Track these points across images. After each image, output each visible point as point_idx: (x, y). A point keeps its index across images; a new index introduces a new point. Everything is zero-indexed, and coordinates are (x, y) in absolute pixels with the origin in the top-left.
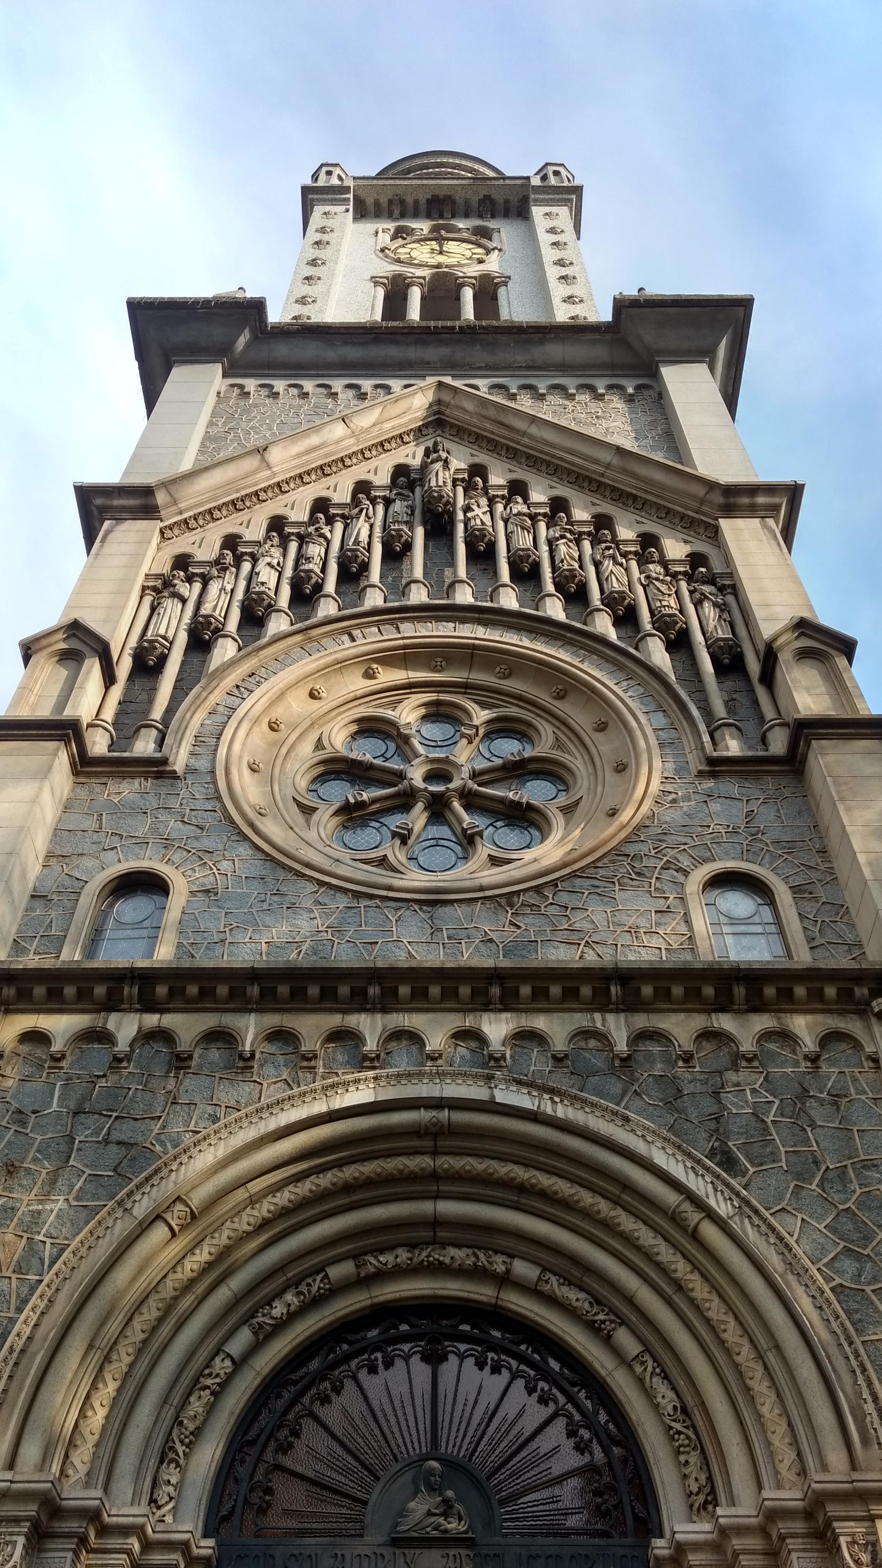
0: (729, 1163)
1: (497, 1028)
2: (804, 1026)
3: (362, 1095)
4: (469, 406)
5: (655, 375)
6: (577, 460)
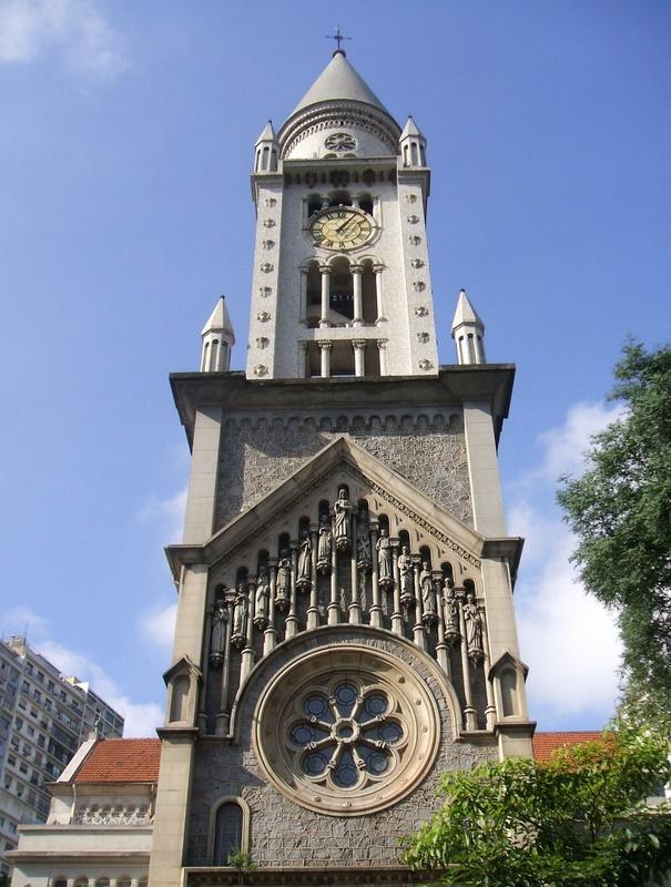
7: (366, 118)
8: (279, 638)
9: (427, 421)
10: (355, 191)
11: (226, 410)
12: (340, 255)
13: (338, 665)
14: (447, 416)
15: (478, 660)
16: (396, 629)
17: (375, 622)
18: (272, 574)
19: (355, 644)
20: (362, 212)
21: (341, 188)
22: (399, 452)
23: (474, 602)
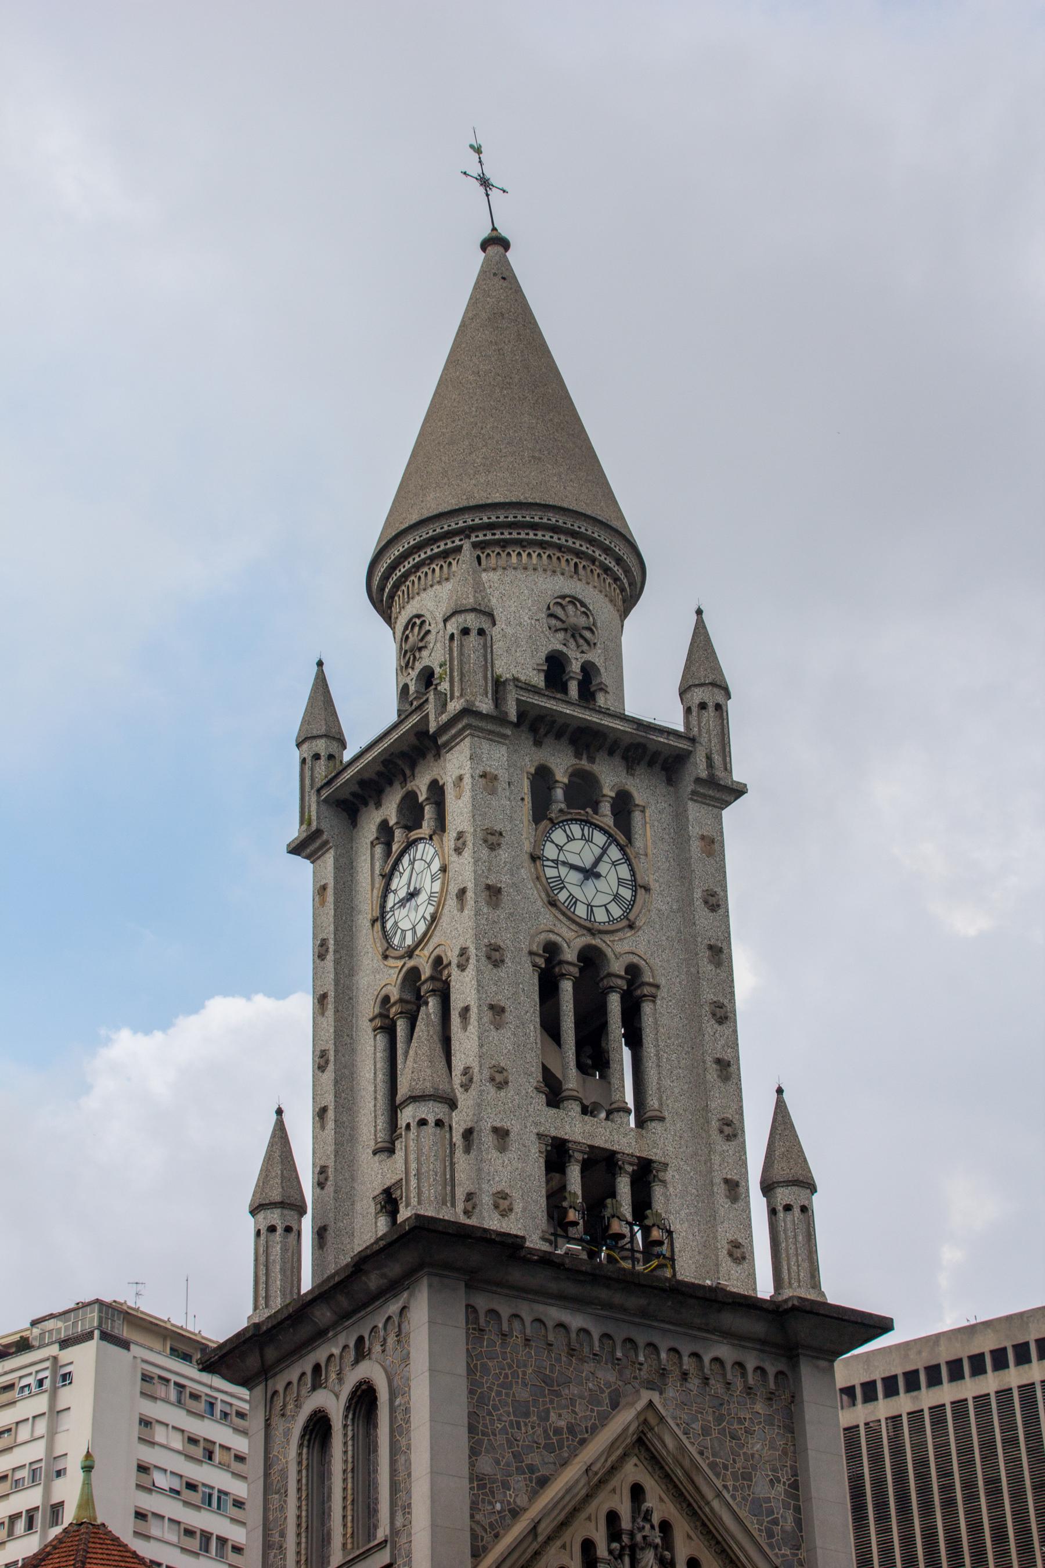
5: (795, 1366)
6: (743, 1558)
7: (612, 564)
9: (744, 1374)
10: (610, 778)
11: (469, 1286)
14: (771, 1370)
20: (622, 839)
21: (584, 763)
22: (706, 1431)
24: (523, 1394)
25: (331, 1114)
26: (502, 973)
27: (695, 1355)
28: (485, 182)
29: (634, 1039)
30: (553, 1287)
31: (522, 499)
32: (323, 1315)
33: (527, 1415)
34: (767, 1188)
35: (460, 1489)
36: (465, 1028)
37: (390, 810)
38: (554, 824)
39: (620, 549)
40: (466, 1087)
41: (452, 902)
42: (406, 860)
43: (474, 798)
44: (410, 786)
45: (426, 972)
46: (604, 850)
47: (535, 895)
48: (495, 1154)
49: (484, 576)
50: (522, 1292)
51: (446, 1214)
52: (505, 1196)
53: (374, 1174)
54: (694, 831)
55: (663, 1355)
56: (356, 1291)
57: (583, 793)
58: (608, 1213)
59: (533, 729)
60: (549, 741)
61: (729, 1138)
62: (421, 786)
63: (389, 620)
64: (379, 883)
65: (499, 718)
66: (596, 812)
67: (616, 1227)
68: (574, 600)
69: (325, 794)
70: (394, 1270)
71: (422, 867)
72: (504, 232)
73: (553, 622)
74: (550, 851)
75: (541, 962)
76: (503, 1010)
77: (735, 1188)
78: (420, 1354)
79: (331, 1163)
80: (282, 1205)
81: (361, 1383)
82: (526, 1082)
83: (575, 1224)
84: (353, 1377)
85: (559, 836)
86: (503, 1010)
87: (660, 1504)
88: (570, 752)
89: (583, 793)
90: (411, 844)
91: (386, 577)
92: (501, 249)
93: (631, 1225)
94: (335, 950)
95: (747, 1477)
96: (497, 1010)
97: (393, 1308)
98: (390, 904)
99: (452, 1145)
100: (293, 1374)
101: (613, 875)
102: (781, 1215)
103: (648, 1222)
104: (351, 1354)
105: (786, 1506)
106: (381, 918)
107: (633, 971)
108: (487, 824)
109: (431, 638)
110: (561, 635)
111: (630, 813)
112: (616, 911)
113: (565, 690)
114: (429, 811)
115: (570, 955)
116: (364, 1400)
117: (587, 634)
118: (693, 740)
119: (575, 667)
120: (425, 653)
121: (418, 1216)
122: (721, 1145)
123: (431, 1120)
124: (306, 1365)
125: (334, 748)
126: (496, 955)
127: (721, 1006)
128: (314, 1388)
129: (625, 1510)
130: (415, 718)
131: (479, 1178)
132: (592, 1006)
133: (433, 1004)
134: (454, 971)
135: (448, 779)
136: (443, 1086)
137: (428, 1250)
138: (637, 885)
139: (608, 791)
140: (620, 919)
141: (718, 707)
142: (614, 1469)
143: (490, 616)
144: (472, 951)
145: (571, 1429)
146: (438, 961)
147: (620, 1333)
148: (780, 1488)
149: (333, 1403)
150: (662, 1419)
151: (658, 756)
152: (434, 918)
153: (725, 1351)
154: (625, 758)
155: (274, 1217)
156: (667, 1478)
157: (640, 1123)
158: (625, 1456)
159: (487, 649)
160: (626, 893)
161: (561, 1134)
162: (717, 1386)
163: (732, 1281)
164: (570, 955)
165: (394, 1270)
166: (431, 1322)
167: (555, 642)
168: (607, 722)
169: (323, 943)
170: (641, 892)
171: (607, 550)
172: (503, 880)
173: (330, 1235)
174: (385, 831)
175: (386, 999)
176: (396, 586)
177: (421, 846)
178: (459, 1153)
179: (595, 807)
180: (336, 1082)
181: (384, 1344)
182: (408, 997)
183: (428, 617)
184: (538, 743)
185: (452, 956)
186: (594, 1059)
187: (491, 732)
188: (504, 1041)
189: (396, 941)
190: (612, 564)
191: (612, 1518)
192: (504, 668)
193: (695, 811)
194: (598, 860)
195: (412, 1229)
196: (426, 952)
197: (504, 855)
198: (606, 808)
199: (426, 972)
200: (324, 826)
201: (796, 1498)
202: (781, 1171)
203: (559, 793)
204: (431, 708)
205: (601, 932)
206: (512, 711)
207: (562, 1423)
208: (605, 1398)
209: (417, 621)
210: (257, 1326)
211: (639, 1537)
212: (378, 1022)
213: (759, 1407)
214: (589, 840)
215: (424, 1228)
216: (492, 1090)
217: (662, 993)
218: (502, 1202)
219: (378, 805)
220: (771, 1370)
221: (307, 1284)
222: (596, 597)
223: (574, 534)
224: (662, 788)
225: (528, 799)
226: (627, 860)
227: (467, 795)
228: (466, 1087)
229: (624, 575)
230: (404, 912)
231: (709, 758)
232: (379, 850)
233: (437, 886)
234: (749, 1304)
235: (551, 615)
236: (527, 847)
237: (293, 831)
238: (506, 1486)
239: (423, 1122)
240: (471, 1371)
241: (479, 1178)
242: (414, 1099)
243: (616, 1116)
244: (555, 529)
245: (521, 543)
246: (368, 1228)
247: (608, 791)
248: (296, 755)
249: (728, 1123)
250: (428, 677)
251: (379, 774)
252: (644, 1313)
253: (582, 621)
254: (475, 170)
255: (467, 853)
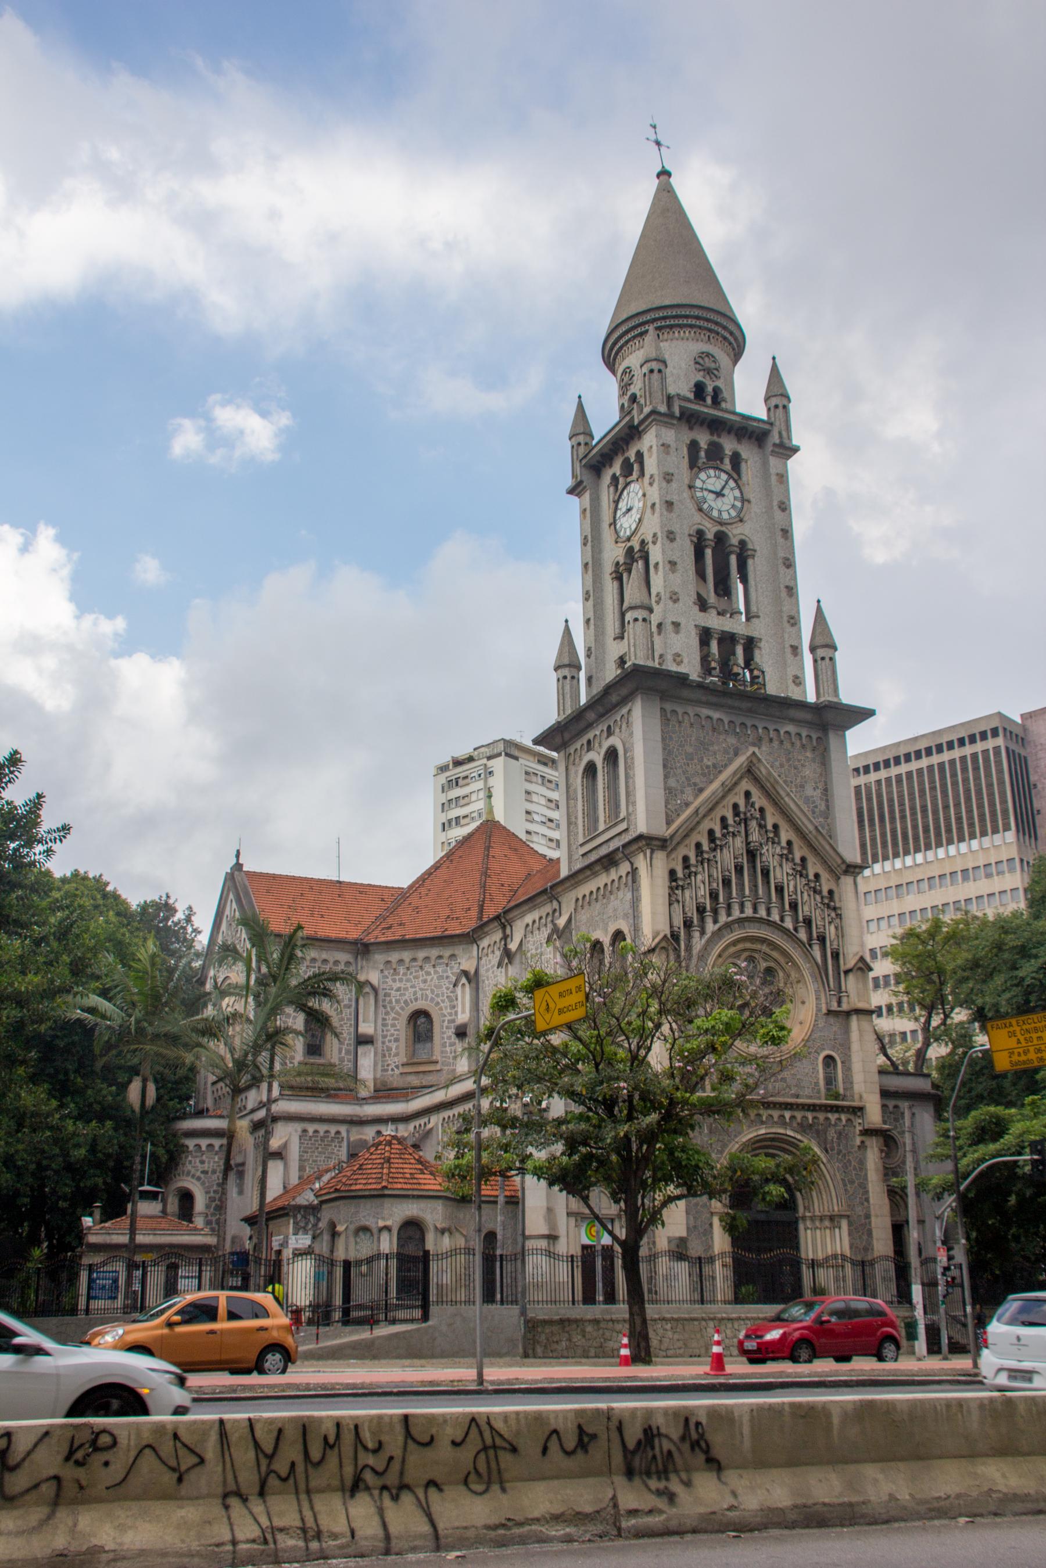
0: (827, 1151)
1: (787, 1114)
2: (843, 1117)
3: (763, 1131)
4: (764, 771)
5: (826, 734)
7: (728, 336)
8: (715, 921)
9: (801, 738)
10: (729, 445)
11: (661, 699)
12: (718, 528)
13: (748, 945)
14: (814, 736)
15: (836, 955)
16: (789, 924)
17: (762, 913)
18: (706, 865)
19: (753, 931)
20: (735, 476)
21: (715, 438)
22: (782, 766)
23: (835, 909)
24: (690, 750)
25: (592, 622)
26: (675, 545)
27: (776, 730)
28: (658, 143)
29: (744, 580)
30: (704, 698)
31: (680, 302)
32: (591, 716)
33: (692, 759)
34: (813, 649)
35: (660, 794)
36: (656, 573)
37: (616, 468)
38: (700, 470)
39: (732, 327)
40: (658, 602)
41: (649, 510)
42: (625, 493)
43: (658, 457)
44: (626, 455)
45: (637, 548)
46: (727, 482)
47: (691, 506)
48: (673, 635)
49: (662, 344)
50: (689, 701)
51: (650, 663)
52: (679, 655)
53: (614, 650)
54: (773, 471)
55: (760, 731)
56: (607, 703)
57: (715, 453)
58: (731, 663)
59: (688, 421)
60: (696, 427)
61: (793, 625)
62: (632, 454)
63: (613, 371)
64: (612, 505)
65: (670, 415)
66: (722, 462)
67: (736, 670)
68: (708, 355)
69: (584, 462)
70: (624, 691)
71: (634, 496)
72: (668, 168)
73: (698, 366)
74: (698, 484)
75: (695, 539)
76: (675, 563)
77: (796, 650)
78: (638, 731)
79: (593, 645)
80: (569, 666)
81: (610, 747)
82: (688, 599)
83: (715, 669)
84: (606, 745)
85: (703, 475)
86: (675, 563)
87: (758, 799)
88: (708, 433)
89: (715, 453)
90: (627, 484)
91: (611, 349)
92: (666, 177)
93: (743, 669)
94: (592, 541)
95: (802, 786)
96: (673, 564)
97: (624, 711)
98: (618, 515)
99: (652, 633)
100: (578, 745)
101: (731, 495)
102: (819, 662)
103: (752, 667)
104: (605, 734)
105: (822, 799)
106: (614, 523)
107: (743, 543)
108: (666, 470)
109: (635, 378)
110: (702, 373)
111: (739, 463)
112: (733, 513)
113: (704, 400)
114: (636, 467)
115: (710, 536)
116: (612, 755)
117: (715, 372)
118: (771, 424)
119: (710, 389)
120: (632, 386)
121: (634, 665)
122: (788, 628)
123: (640, 618)
124: (584, 740)
125: (588, 439)
126: (672, 536)
127: (788, 559)
128: (588, 750)
129: (742, 803)
130: (627, 419)
131: (666, 647)
132: (720, 561)
133: (641, 563)
134: (651, 545)
135: (645, 450)
136: (646, 601)
137: (641, 681)
138: (743, 500)
139: (728, 452)
140: (735, 517)
141: (784, 407)
142: (736, 784)
143: (664, 362)
144: (659, 535)
145: (714, 766)
146: (643, 541)
147: (738, 720)
148: (819, 791)
149: (597, 757)
150: (759, 760)
151: (753, 433)
152: (640, 520)
153: (791, 728)
154: (736, 435)
155: (566, 672)
156: (762, 788)
157: (748, 619)
158: (741, 778)
159: (663, 380)
160: (738, 504)
161: (707, 625)
162: (787, 745)
163: (794, 694)
164: (710, 536)
165: (624, 691)
166: (643, 716)
167: (699, 377)
168: (726, 416)
169: (586, 538)
170: (746, 503)
171: (725, 328)
172: (674, 498)
173: (594, 680)
174: (615, 479)
175: (618, 563)
176: (617, 354)
177: (632, 485)
178: (655, 635)
179: (722, 460)
180: (594, 606)
181: (620, 728)
182: (628, 561)
183: (633, 368)
184: (691, 428)
185: (649, 538)
186: (724, 589)
187: (666, 423)
188: (676, 579)
189: (622, 534)
190: (728, 336)
191: (735, 806)
192: (672, 390)
193: (773, 461)
194: (723, 488)
195: (632, 671)
196: (637, 538)
197: (674, 485)
198: (727, 461)
199: (637, 548)
200: (584, 478)
201: (826, 795)
202: (819, 641)
203: (702, 454)
204: (635, 412)
205: (726, 524)
206: (677, 412)
207: (710, 763)
208: (732, 752)
209: (628, 371)
210: (559, 723)
211: (748, 815)
212: (614, 575)
213: (809, 754)
214: (719, 478)
215: (637, 669)
216: (670, 603)
217: (758, 554)
218: (677, 658)
219: (611, 466)
220: (814, 736)
221: (583, 700)
222: (723, 358)
223: (708, 320)
224: (756, 450)
225: (686, 457)
226: (739, 487)
227: (655, 455)
228: (658, 602)
229: (735, 343)
230: (625, 519)
231: (780, 433)
232: (612, 489)
233: (641, 504)
234: (803, 705)
235: (697, 363)
236: (687, 481)
237: (569, 482)
238: (682, 792)
239: (636, 620)
240: (663, 739)
241: (666, 647)
242: (631, 608)
243: (735, 616)
244: (697, 318)
245: (681, 326)
246: (611, 673)
247: (728, 452)
248: (569, 444)
249: (792, 618)
250: (633, 399)
251: (610, 450)
252: (750, 710)
253: (713, 365)
254: (653, 137)
255: (656, 485)
